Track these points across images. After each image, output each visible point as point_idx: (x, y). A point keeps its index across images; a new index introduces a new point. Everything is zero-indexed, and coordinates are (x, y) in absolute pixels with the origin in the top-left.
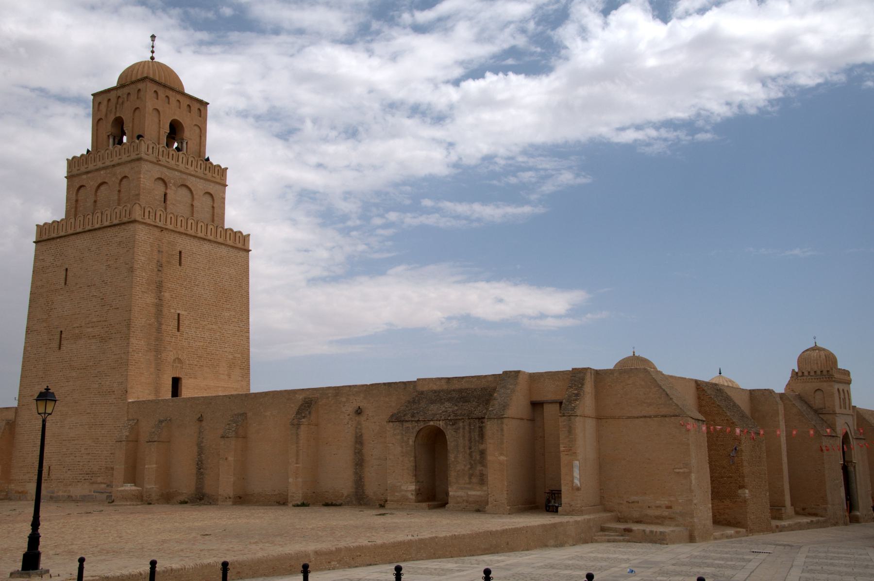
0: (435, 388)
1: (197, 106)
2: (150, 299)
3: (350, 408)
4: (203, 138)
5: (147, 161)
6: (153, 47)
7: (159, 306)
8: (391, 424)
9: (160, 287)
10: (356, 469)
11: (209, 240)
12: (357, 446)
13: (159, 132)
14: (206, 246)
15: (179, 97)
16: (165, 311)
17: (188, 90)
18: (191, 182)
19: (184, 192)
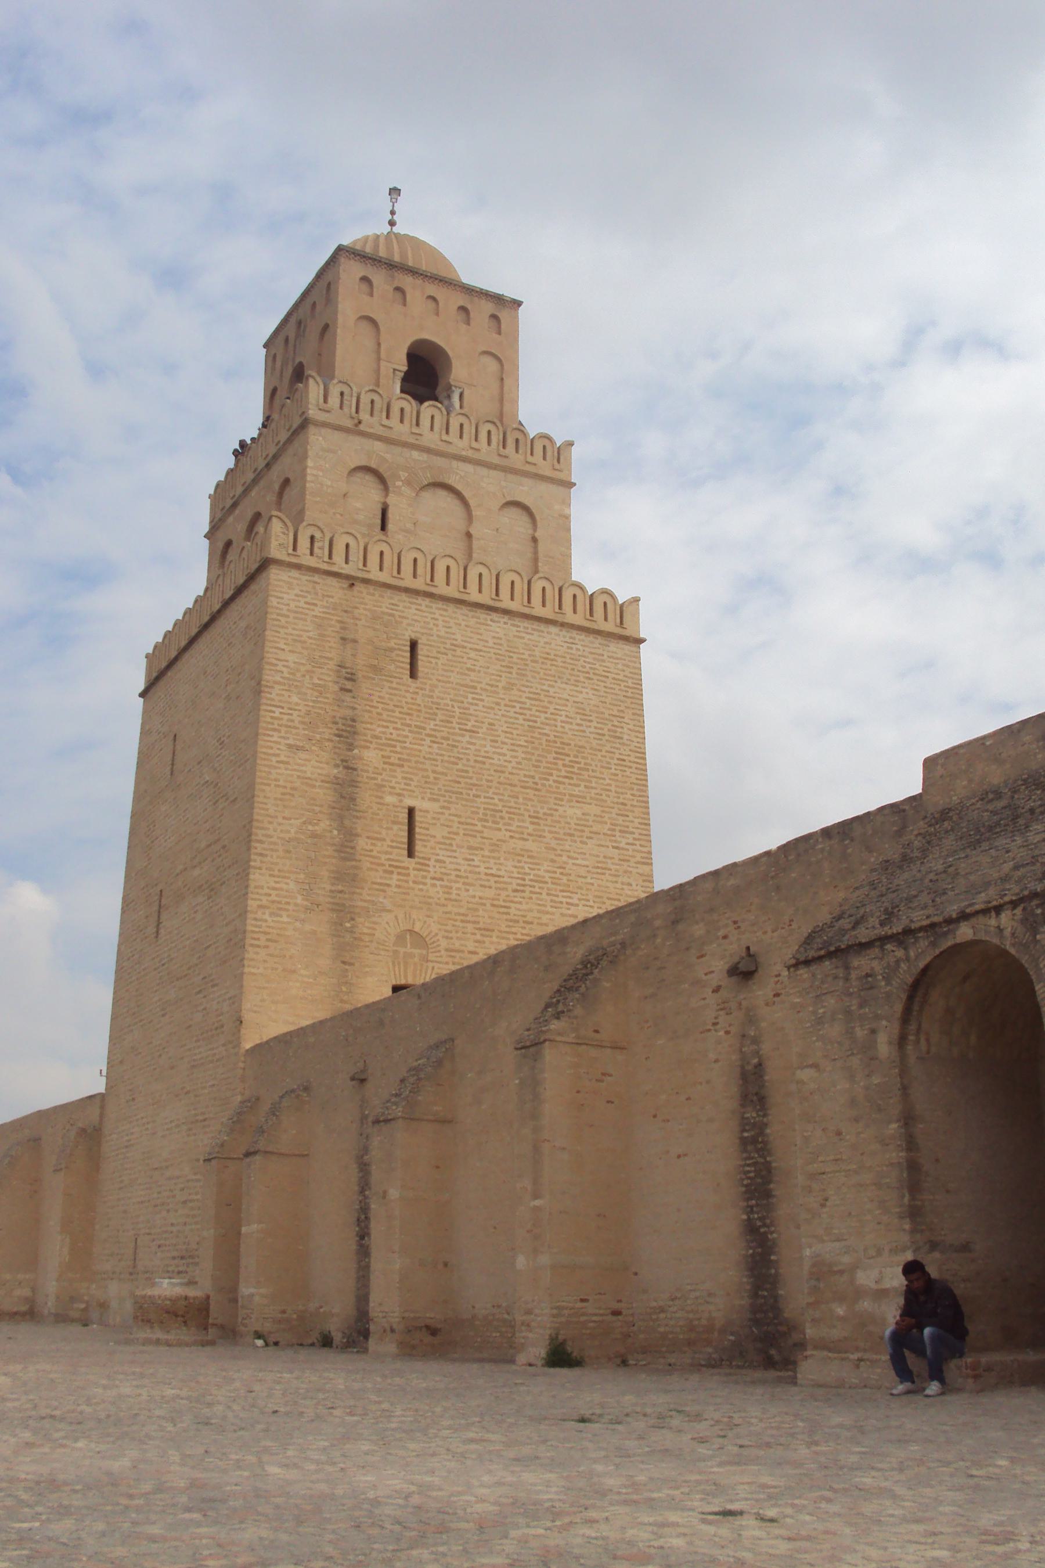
0: (996, 776)
1: (488, 307)
2: (317, 765)
3: (716, 965)
4: (507, 382)
5: (324, 425)
6: (393, 213)
7: (346, 790)
8: (803, 972)
9: (348, 734)
10: (750, 1210)
11: (506, 612)
12: (751, 1114)
13: (378, 371)
14: (499, 627)
15: (432, 289)
16: (366, 799)
17: (466, 279)
18: (459, 475)
19: (443, 500)
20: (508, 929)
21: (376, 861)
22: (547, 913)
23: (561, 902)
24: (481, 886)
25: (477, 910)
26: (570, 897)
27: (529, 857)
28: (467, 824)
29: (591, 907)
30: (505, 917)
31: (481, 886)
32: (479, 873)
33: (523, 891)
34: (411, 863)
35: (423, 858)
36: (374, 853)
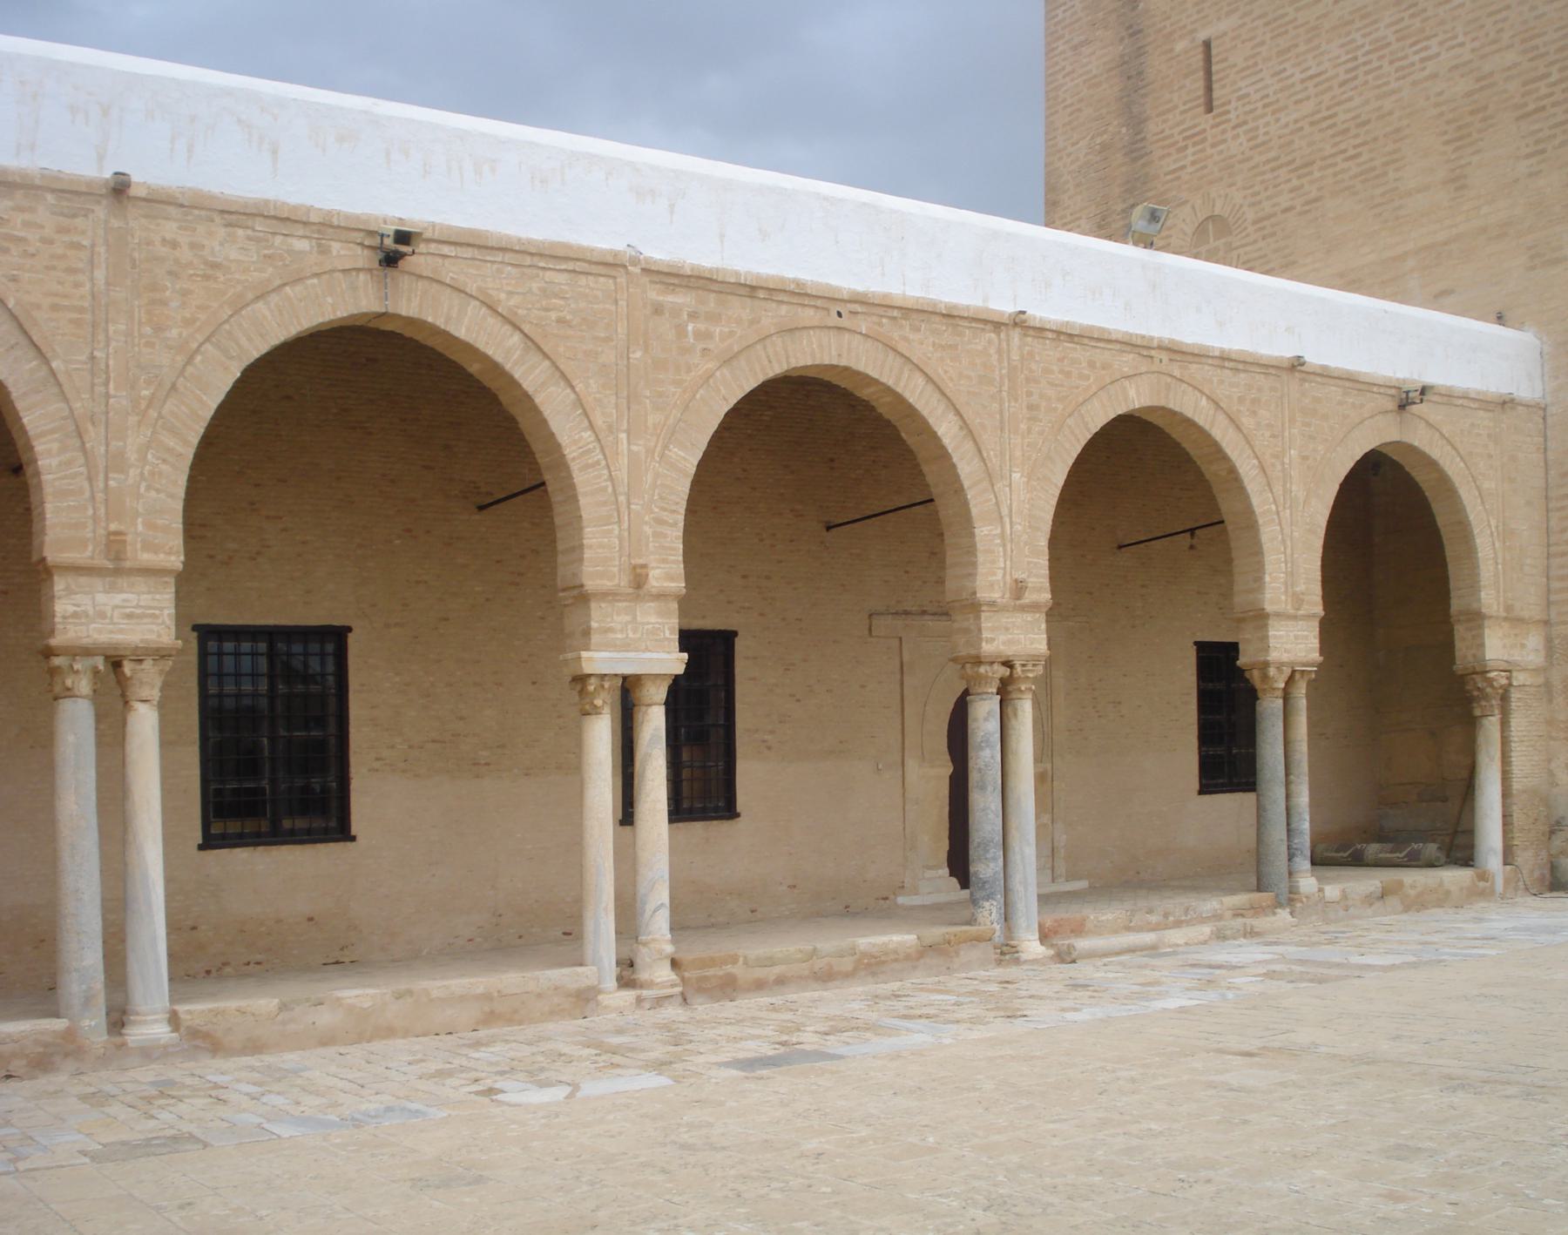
20: (1334, 151)
21: (1167, 142)
22: (1393, 92)
23: (1413, 64)
24: (1296, 102)
25: (1291, 142)
26: (1426, 48)
27: (1363, 17)
28: (1275, 20)
29: (1462, 45)
30: (1330, 132)
31: (1296, 102)
32: (1293, 85)
33: (1355, 78)
34: (1206, 121)
35: (1223, 105)
36: (1168, 132)
